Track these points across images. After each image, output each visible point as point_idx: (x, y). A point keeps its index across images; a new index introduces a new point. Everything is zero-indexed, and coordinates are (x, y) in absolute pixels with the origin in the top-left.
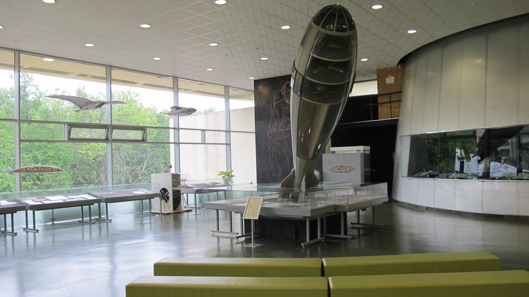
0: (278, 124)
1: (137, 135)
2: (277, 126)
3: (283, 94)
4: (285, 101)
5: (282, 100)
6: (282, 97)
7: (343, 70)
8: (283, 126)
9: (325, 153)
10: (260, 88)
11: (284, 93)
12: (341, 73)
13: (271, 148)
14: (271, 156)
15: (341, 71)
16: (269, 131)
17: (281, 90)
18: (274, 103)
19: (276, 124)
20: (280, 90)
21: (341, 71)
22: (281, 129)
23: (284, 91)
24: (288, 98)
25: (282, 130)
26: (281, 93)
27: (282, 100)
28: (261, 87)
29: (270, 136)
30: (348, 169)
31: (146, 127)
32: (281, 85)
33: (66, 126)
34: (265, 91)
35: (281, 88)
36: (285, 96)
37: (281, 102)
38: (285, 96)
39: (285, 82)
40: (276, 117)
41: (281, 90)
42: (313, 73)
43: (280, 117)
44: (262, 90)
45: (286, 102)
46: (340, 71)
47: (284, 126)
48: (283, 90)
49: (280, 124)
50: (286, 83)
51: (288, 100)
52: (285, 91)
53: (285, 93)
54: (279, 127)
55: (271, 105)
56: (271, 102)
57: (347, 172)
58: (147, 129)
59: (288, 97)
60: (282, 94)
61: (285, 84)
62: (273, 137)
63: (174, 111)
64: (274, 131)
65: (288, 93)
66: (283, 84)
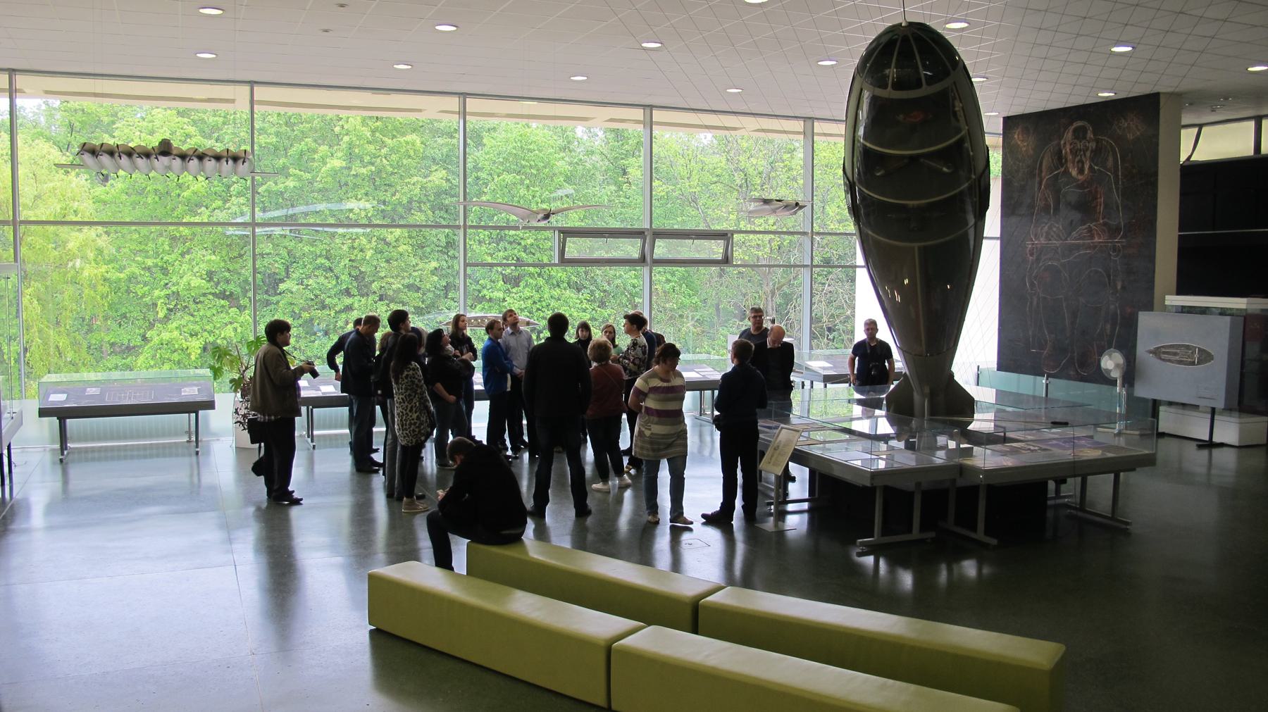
0: (1050, 228)
1: (715, 249)
2: (1048, 233)
3: (1066, 153)
4: (1069, 171)
5: (1063, 169)
6: (1064, 161)
7: (948, 168)
8: (1061, 235)
9: (1149, 307)
10: (1016, 136)
11: (1068, 150)
12: (945, 174)
13: (1032, 285)
14: (1031, 303)
15: (945, 169)
16: (1028, 244)
17: (1062, 142)
18: (1043, 174)
19: (1046, 227)
20: (1060, 143)
21: (945, 169)
22: (1056, 240)
23: (1068, 148)
25: (1057, 243)
27: (1062, 167)
28: (1018, 135)
29: (1032, 254)
30: (1196, 356)
31: (733, 232)
32: (1062, 130)
33: (557, 232)
34: (1025, 144)
35: (1060, 137)
36: (1070, 157)
37: (1059, 173)
38: (1070, 157)
39: (1071, 124)
40: (1046, 209)
41: (1062, 142)
42: (878, 176)
43: (1057, 209)
44: (1019, 143)
45: (1070, 174)
46: (942, 169)
47: (1063, 234)
48: (1065, 143)
49: (1055, 227)
50: (1072, 125)
52: (1071, 144)
53: (1070, 150)
54: (1052, 236)
55: (1037, 179)
56: (1037, 171)
57: (1193, 363)
58: (735, 236)
59: (1076, 160)
60: (1063, 152)
61: (1072, 128)
62: (1038, 260)
63: (761, 205)
64: (1041, 244)
65: (1076, 152)
66: (1066, 128)
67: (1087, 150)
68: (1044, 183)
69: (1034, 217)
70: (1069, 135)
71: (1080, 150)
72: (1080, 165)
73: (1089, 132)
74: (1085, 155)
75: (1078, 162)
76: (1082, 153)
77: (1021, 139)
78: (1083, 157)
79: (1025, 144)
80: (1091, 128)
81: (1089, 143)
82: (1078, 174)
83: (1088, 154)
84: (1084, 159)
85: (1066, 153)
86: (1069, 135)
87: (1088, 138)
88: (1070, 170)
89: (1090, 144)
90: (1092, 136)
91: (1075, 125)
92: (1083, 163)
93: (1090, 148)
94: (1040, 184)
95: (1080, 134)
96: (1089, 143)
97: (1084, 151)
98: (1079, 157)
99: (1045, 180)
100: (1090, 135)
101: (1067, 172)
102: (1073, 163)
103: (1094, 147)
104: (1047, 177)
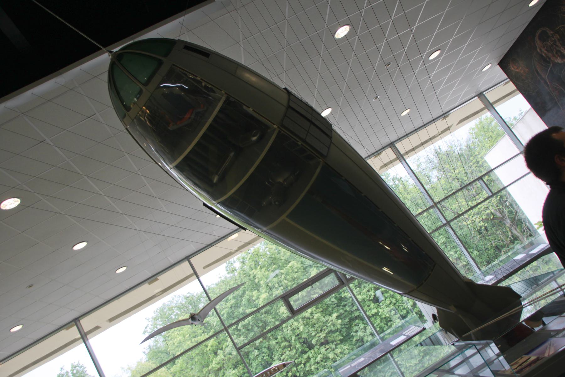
3: (546, 54)
5: (551, 65)
10: (512, 69)
11: (546, 52)
17: (539, 50)
18: (543, 76)
23: (543, 50)
24: (556, 55)
26: (542, 56)
27: (550, 63)
37: (551, 68)
38: (550, 55)
41: (539, 50)
45: (558, 63)
48: (540, 50)
51: (559, 58)
52: (544, 47)
53: (546, 50)
59: (554, 53)
61: (537, 38)
67: (556, 43)
68: (547, 81)
69: (559, 104)
70: (538, 43)
71: (552, 46)
72: (559, 54)
73: (548, 31)
74: (557, 46)
75: (556, 53)
76: (554, 46)
77: (516, 67)
78: (556, 48)
79: (520, 68)
80: (548, 29)
81: (553, 37)
82: (562, 60)
83: (558, 44)
84: (558, 48)
85: (546, 54)
86: (538, 43)
87: (551, 35)
88: (556, 61)
89: (555, 37)
90: (552, 32)
91: (537, 35)
92: (560, 51)
93: (556, 39)
94: (546, 83)
95: (544, 38)
96: (553, 37)
97: (554, 44)
98: (555, 50)
99: (547, 78)
100: (550, 33)
101: (555, 64)
102: (554, 56)
103: (558, 37)
104: (547, 76)
